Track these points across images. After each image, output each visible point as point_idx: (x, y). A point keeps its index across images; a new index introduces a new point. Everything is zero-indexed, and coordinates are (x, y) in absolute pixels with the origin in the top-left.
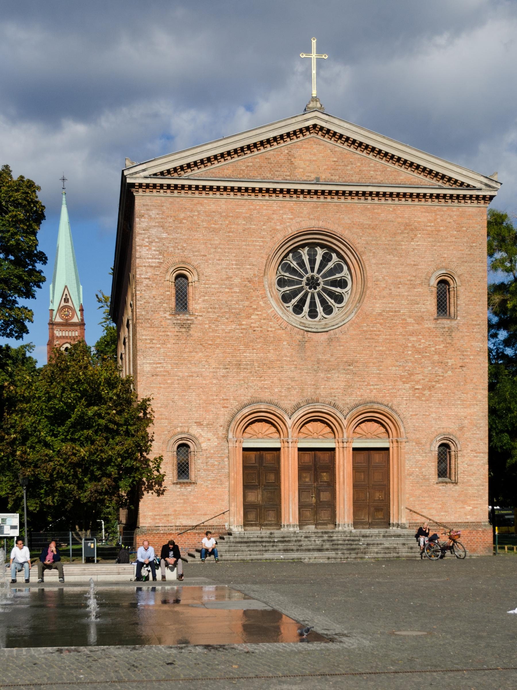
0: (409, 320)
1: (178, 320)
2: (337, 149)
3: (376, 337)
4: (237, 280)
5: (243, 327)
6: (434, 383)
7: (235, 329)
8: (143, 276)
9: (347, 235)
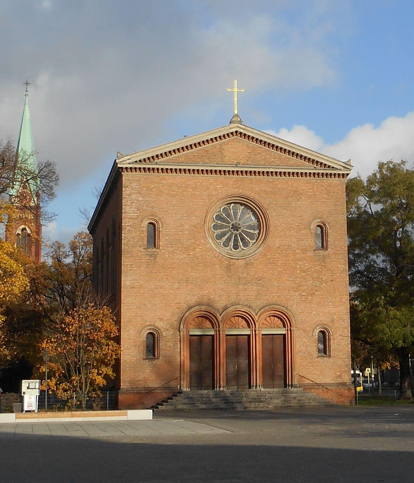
0: (297, 251)
2: (250, 145)
3: (276, 262)
4: (187, 227)
5: (190, 256)
6: (314, 292)
7: (185, 258)
8: (126, 225)
9: (257, 198)
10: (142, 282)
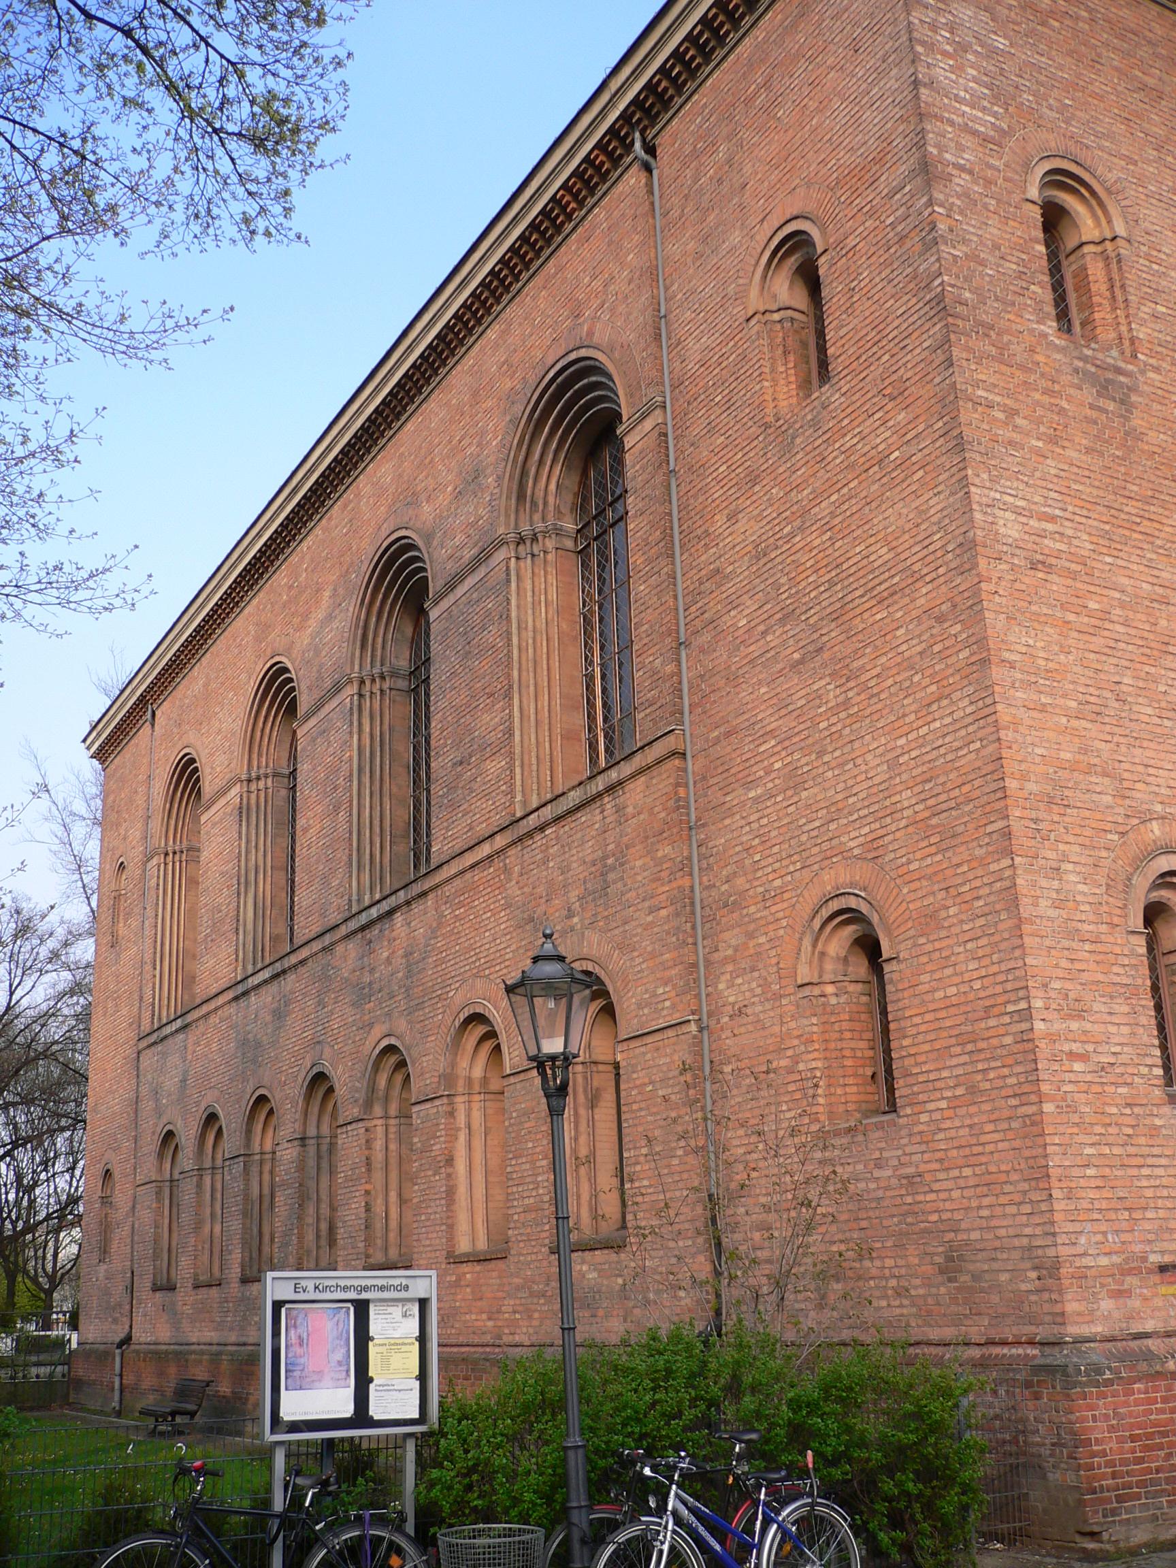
1: (1085, 359)
10: (1085, 545)
